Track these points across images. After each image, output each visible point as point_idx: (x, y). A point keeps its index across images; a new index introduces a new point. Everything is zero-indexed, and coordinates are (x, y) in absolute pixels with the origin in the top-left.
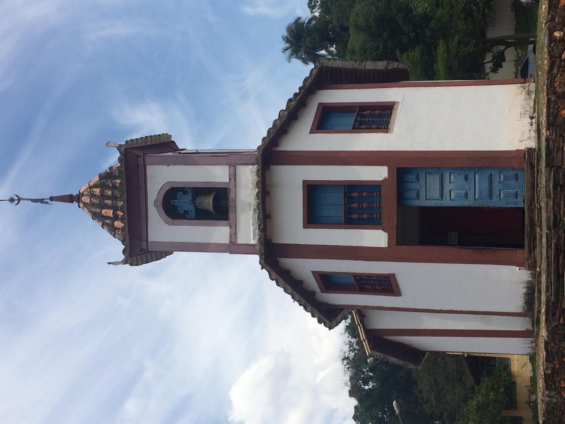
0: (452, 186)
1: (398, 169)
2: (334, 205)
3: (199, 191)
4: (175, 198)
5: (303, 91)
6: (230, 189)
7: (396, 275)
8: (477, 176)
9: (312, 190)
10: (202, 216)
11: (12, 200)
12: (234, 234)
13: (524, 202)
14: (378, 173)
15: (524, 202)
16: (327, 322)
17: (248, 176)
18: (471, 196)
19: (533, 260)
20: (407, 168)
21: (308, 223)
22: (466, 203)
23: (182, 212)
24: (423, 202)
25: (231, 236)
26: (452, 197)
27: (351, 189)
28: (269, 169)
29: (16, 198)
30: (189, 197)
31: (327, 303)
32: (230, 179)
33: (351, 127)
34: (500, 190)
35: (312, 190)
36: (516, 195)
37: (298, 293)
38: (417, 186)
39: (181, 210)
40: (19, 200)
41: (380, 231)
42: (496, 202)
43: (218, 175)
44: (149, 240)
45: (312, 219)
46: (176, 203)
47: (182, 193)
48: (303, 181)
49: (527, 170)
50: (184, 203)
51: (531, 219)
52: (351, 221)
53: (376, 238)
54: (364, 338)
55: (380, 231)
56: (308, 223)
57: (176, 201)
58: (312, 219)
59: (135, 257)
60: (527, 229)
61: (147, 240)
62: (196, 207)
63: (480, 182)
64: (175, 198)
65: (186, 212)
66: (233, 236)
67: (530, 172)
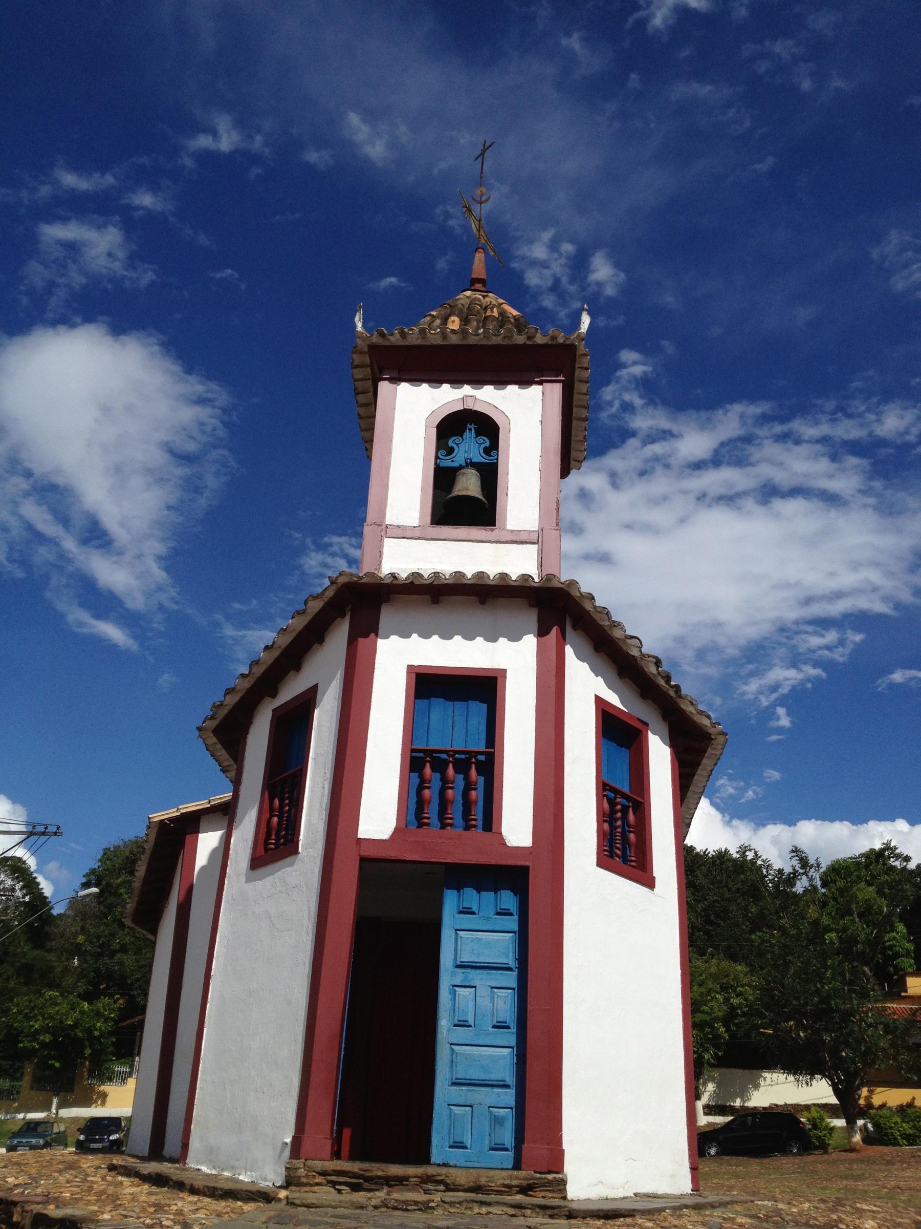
2: (455, 728)
3: (490, 475)
5: (672, 693)
6: (492, 530)
9: (484, 688)
10: (443, 478)
12: (404, 533)
13: (445, 1165)
14: (517, 827)
15: (445, 1165)
16: (214, 724)
17: (520, 563)
18: (462, 1034)
19: (304, 1180)
20: (526, 887)
21: (417, 674)
22: (444, 1022)
23: (451, 444)
25: (399, 527)
27: (486, 765)
28: (531, 605)
30: (478, 457)
31: (251, 723)
32: (512, 531)
33: (605, 779)
34: (471, 1106)
35: (484, 688)
36: (458, 1145)
37: (277, 660)
39: (454, 441)
41: (395, 824)
45: (427, 685)
46: (470, 435)
47: (488, 444)
48: (505, 671)
49: (517, 1178)
50: (469, 447)
51: (401, 1181)
52: (418, 761)
53: (379, 814)
54: (183, 811)
58: (427, 685)
59: (367, 359)
60: (378, 1169)
62: (461, 467)
63: (499, 1059)
65: (450, 451)
67: (515, 1182)
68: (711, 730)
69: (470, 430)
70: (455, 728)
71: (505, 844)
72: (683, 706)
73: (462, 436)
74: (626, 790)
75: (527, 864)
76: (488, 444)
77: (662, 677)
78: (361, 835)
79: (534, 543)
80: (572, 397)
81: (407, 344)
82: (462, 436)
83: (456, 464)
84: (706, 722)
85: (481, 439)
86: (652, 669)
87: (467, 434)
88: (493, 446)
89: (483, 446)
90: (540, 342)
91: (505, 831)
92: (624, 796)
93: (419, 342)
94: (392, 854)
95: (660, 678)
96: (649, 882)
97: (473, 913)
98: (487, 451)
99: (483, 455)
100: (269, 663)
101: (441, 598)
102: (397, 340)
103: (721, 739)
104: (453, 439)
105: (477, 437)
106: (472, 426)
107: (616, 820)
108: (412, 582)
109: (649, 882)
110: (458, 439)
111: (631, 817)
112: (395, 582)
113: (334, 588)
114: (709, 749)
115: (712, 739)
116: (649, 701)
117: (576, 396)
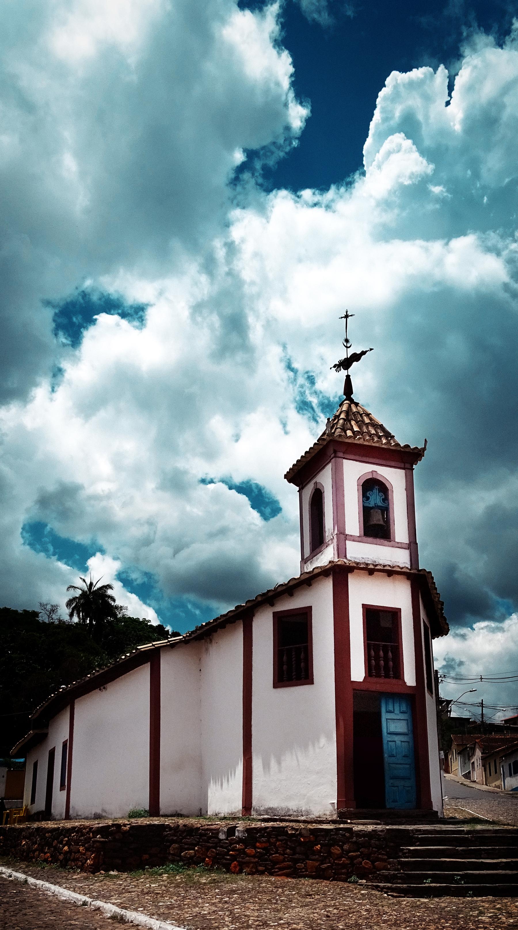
0: (398, 743)
7: (312, 686)
8: (408, 766)
10: (367, 512)
11: (347, 341)
12: (353, 539)
14: (409, 678)
17: (400, 558)
18: (392, 760)
21: (367, 609)
23: (368, 495)
24: (384, 716)
25: (351, 536)
26: (390, 743)
29: (348, 345)
30: (380, 503)
32: (398, 543)
34: (398, 787)
36: (395, 801)
38: (397, 711)
39: (369, 494)
40: (347, 347)
42: (388, 782)
43: (400, 531)
44: (344, 461)
46: (376, 491)
53: (358, 672)
56: (397, 613)
58: (371, 613)
61: (344, 458)
65: (368, 498)
66: (352, 538)
76: (384, 497)
78: (352, 680)
83: (371, 506)
87: (375, 491)
91: (406, 680)
97: (392, 712)
106: (377, 487)
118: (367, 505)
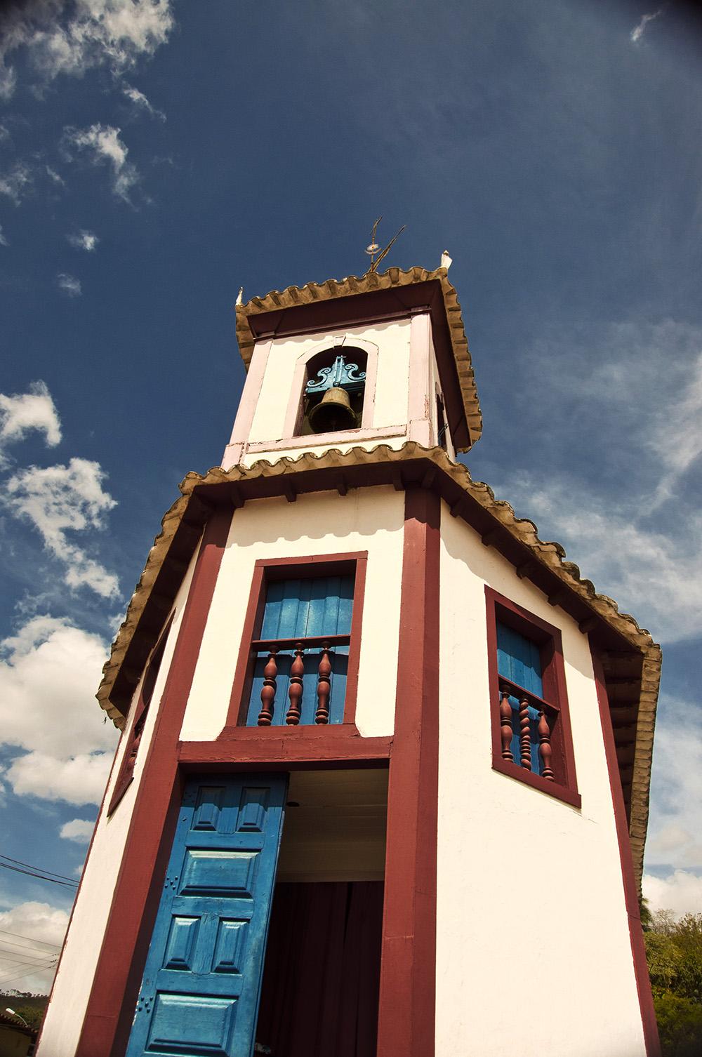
1: (383, 764)
4: (346, 362)
9: (340, 576)
14: (375, 715)
16: (109, 689)
23: (319, 374)
28: (398, 489)
41: (223, 724)
45: (277, 581)
47: (356, 367)
50: (339, 374)
52: (260, 657)
55: (222, 723)
57: (342, 363)
58: (277, 581)
64: (346, 362)
68: (640, 642)
69: (339, 360)
70: (304, 619)
71: (358, 735)
72: (601, 611)
73: (331, 367)
74: (538, 695)
75: (386, 755)
77: (569, 572)
79: (402, 436)
80: (452, 355)
81: (281, 308)
82: (331, 367)
84: (631, 628)
85: (349, 367)
86: (554, 561)
88: (363, 368)
89: (351, 371)
90: (404, 284)
92: (534, 702)
93: (292, 304)
94: (218, 758)
95: (566, 574)
96: (574, 800)
98: (355, 374)
99: (352, 377)
100: (144, 606)
101: (299, 495)
102: (271, 306)
103: (653, 654)
104: (322, 370)
105: (346, 365)
107: (523, 726)
108: (262, 476)
109: (574, 800)
110: (327, 370)
111: (544, 724)
112: (243, 478)
113: (186, 498)
114: (644, 676)
115: (643, 655)
116: (557, 605)
117: (454, 346)
118: (314, 388)
